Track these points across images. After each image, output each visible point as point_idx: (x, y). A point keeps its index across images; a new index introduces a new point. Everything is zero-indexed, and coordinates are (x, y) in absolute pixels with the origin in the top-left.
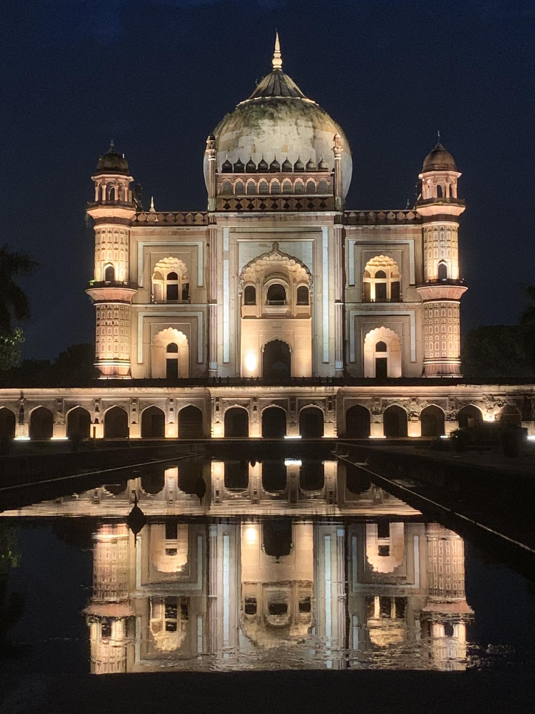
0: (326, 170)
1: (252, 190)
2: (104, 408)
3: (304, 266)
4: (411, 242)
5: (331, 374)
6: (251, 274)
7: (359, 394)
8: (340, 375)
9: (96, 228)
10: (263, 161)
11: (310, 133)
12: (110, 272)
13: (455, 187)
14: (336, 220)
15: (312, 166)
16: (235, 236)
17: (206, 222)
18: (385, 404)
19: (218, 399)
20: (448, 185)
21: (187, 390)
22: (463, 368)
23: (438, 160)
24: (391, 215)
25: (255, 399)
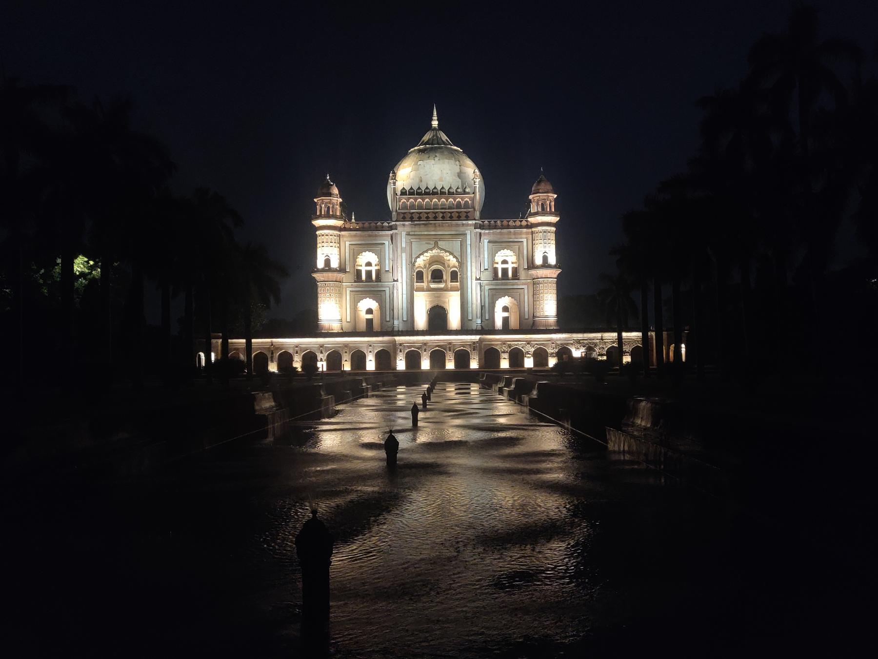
0: (468, 193)
1: (420, 207)
2: (326, 351)
3: (455, 257)
4: (525, 241)
5: (474, 328)
6: (420, 262)
7: (491, 340)
8: (479, 328)
9: (317, 233)
10: (427, 188)
11: (457, 169)
12: (327, 262)
13: (553, 203)
14: (476, 227)
15: (459, 190)
16: (410, 237)
17: (391, 228)
18: (510, 346)
19: (401, 345)
20: (548, 202)
21: (380, 339)
22: (558, 322)
23: (543, 186)
24: (511, 223)
25: (425, 344)
